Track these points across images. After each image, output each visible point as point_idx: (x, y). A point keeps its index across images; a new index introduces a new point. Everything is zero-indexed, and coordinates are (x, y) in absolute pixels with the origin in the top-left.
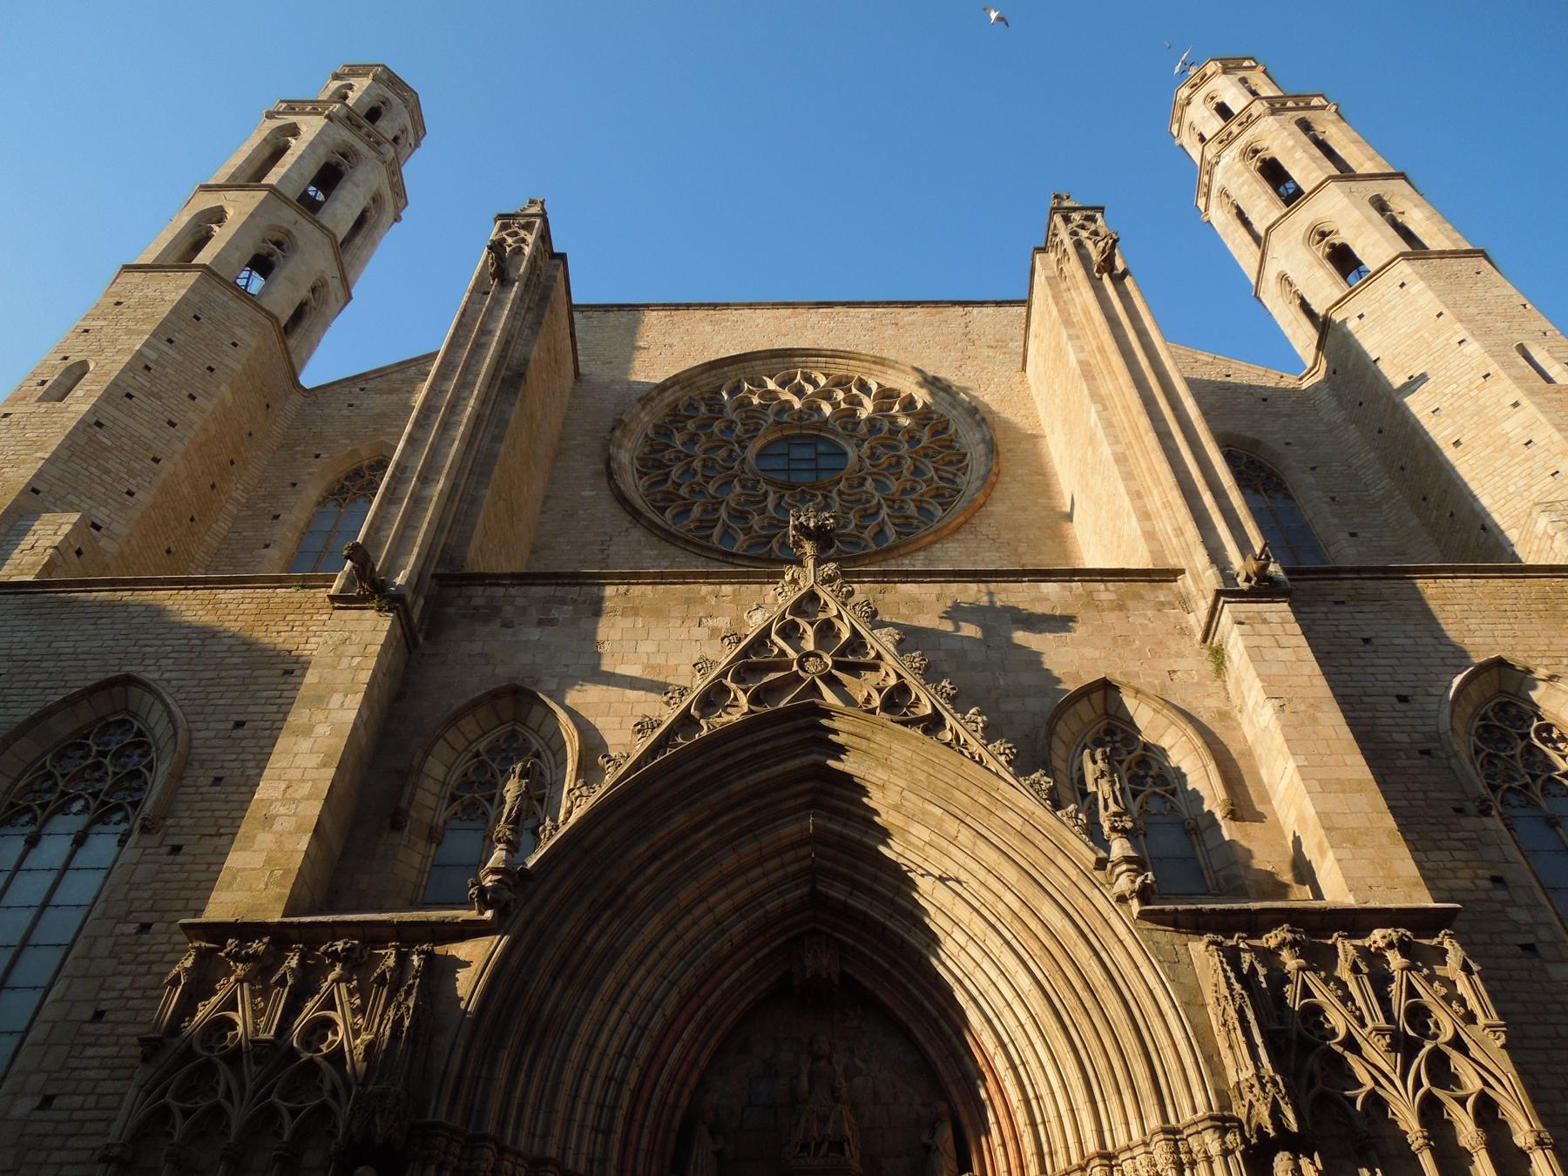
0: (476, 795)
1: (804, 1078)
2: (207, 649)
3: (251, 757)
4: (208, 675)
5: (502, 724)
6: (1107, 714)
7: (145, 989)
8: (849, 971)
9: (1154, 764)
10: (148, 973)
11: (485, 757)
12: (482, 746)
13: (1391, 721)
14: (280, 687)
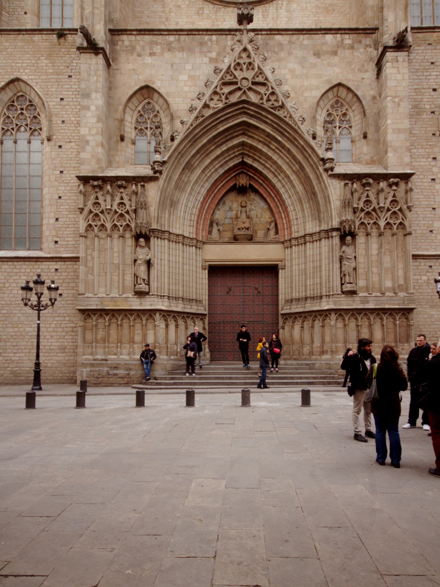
0: (143, 128)
1: (239, 212)
2: (39, 65)
3: (70, 113)
4: (44, 77)
5: (145, 99)
6: (337, 96)
7: (69, 190)
8: (252, 183)
9: (348, 117)
10: (68, 186)
11: (142, 113)
12: (140, 108)
13: (427, 100)
14: (70, 83)
